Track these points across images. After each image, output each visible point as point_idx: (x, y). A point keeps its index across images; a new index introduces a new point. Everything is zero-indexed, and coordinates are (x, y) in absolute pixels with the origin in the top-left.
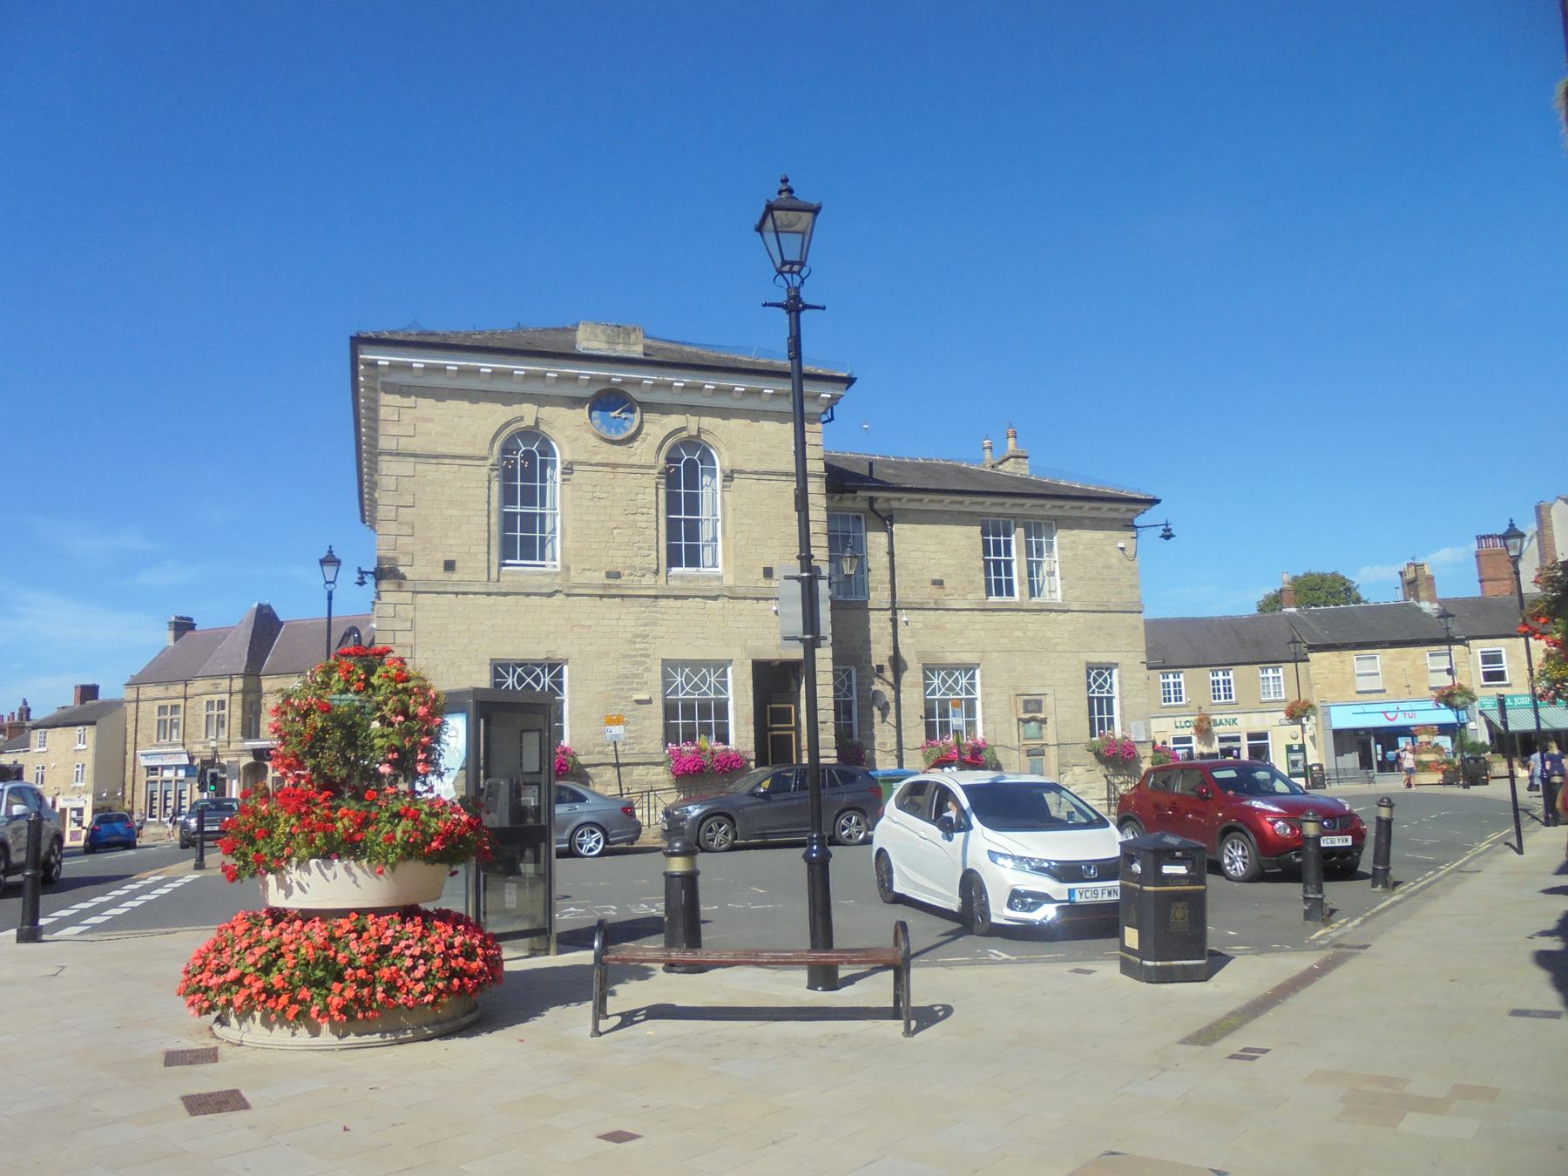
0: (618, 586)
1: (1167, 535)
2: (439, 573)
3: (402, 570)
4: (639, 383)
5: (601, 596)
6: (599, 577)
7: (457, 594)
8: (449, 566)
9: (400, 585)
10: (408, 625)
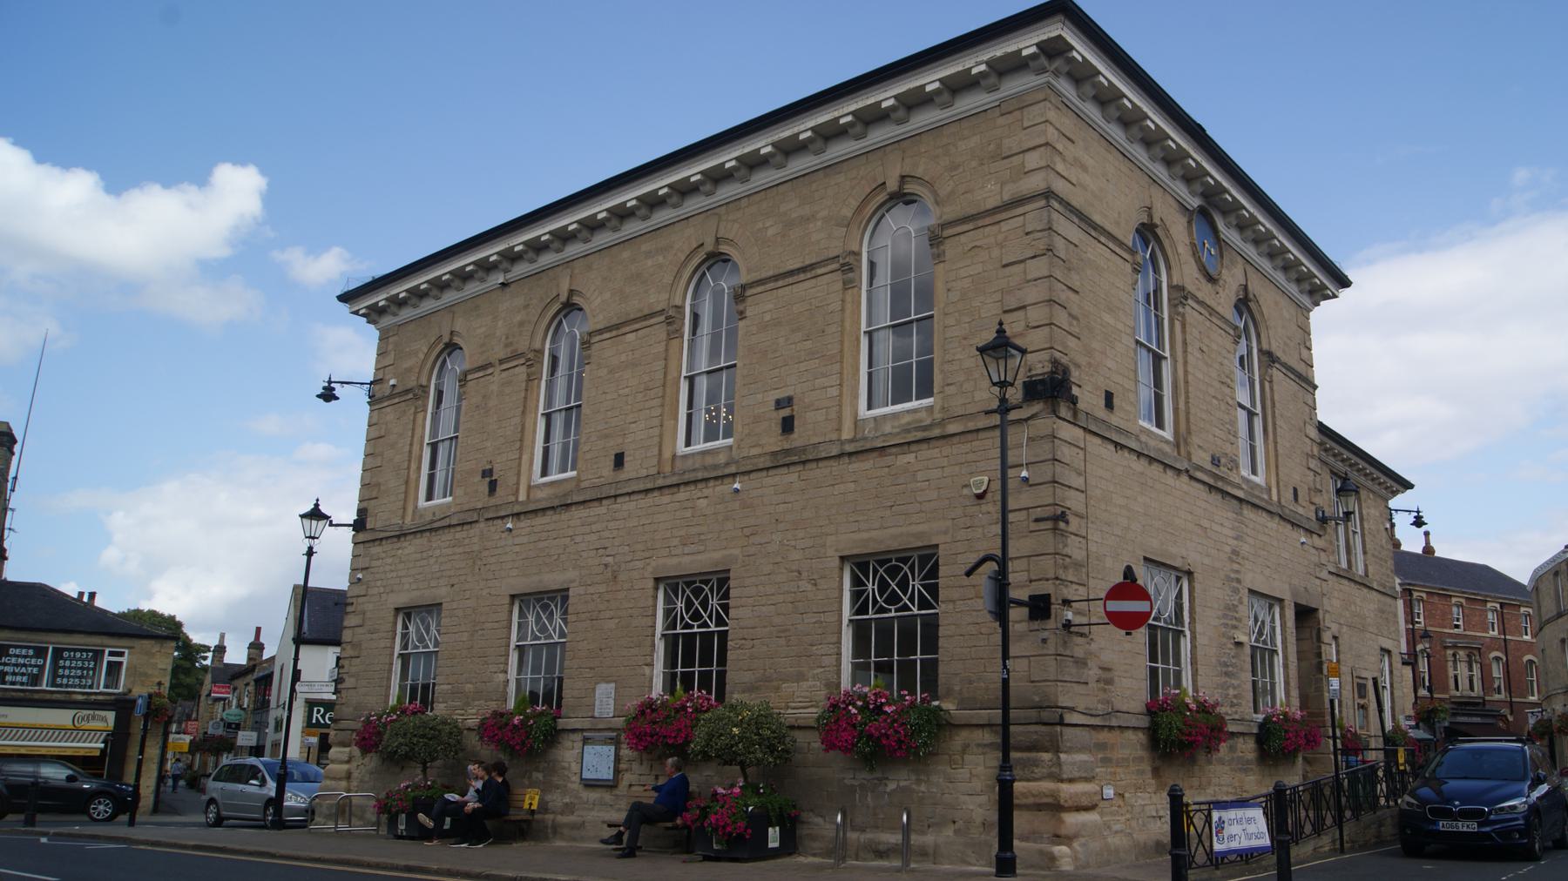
0: (1222, 479)
3: (1075, 391)
4: (1232, 209)
5: (1211, 487)
7: (1116, 444)
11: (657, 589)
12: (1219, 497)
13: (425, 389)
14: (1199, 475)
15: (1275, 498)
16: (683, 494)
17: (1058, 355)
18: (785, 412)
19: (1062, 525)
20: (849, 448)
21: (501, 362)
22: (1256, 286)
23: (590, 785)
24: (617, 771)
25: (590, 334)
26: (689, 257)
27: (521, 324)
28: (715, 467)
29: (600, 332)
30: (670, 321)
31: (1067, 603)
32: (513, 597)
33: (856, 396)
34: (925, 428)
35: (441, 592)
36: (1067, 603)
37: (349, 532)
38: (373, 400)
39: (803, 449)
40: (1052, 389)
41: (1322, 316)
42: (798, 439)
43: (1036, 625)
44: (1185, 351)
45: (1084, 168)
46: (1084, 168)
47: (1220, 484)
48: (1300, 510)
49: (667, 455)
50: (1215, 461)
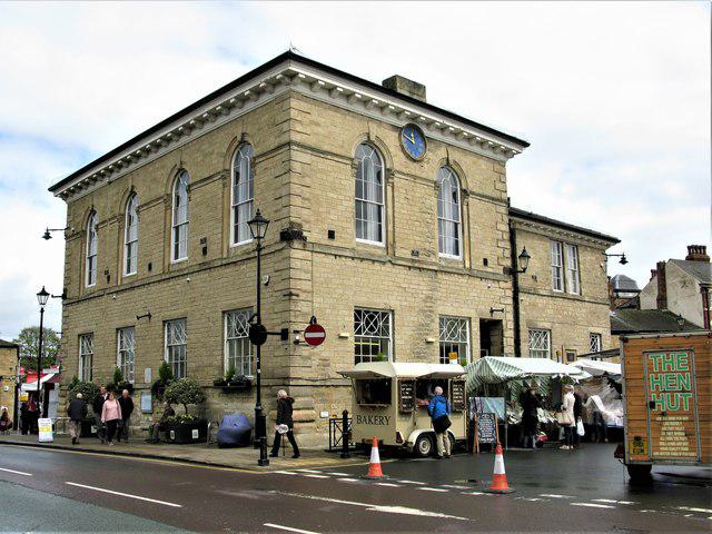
1: (623, 261)
2: (325, 240)
3: (305, 234)
4: (429, 123)
5: (410, 267)
8: (331, 235)
11: (223, 317)
12: (418, 271)
13: (85, 232)
15: (467, 265)
17: (293, 219)
18: (204, 245)
19: (294, 297)
20: (224, 262)
22: (455, 156)
23: (145, 413)
24: (153, 407)
25: (255, 158)
26: (171, 172)
29: (142, 206)
30: (165, 201)
31: (296, 332)
32: (117, 329)
33: (228, 238)
34: (248, 253)
35: (92, 328)
36: (296, 332)
37: (60, 300)
38: (67, 237)
39: (209, 263)
40: (291, 235)
41: (512, 165)
42: (209, 257)
43: (283, 342)
44: (393, 203)
45: (318, 124)
46: (318, 124)
47: (416, 265)
48: (489, 270)
49: (166, 264)
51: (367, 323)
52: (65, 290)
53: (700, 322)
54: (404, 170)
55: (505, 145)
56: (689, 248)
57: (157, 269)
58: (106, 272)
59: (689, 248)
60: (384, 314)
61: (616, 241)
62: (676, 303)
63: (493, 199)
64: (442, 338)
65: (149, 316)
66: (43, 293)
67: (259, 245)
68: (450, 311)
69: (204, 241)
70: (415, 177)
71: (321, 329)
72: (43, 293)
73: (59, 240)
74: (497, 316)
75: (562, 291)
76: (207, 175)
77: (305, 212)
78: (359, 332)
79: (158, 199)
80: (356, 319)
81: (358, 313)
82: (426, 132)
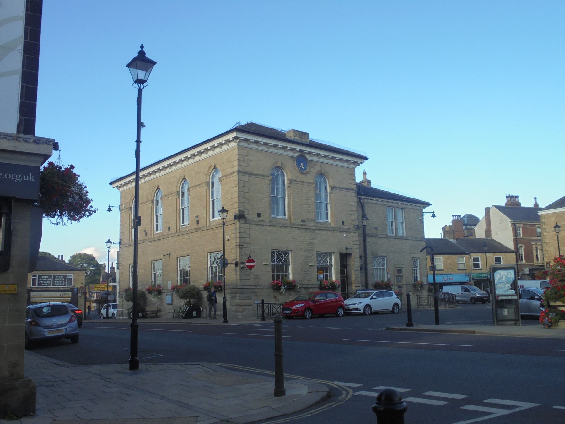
0: (305, 225)
2: (256, 218)
3: (246, 215)
5: (300, 228)
6: (299, 221)
8: (259, 215)
9: (246, 221)
10: (248, 236)
14: (295, 226)
16: (181, 237)
18: (197, 219)
21: (146, 202)
24: (172, 301)
27: (149, 193)
28: (186, 231)
29: (164, 196)
37: (118, 245)
39: (200, 228)
42: (200, 225)
47: (304, 227)
48: (346, 227)
49: (178, 228)
50: (303, 221)
51: (278, 257)
52: (120, 239)
53: (511, 246)
54: (298, 179)
55: (353, 159)
56: (507, 197)
57: (173, 230)
58: (145, 231)
59: (507, 197)
60: (287, 253)
61: (428, 204)
62: (496, 234)
63: (347, 189)
64: (319, 263)
65: (169, 254)
66: (109, 242)
67: (224, 222)
68: (322, 249)
69: (197, 217)
70: (303, 182)
71: (253, 261)
72: (109, 242)
73: (116, 212)
74: (349, 251)
75: (394, 234)
76: (197, 184)
77: (246, 205)
78: (274, 262)
79: (172, 194)
80: (272, 255)
81: (273, 253)
82: (308, 157)
